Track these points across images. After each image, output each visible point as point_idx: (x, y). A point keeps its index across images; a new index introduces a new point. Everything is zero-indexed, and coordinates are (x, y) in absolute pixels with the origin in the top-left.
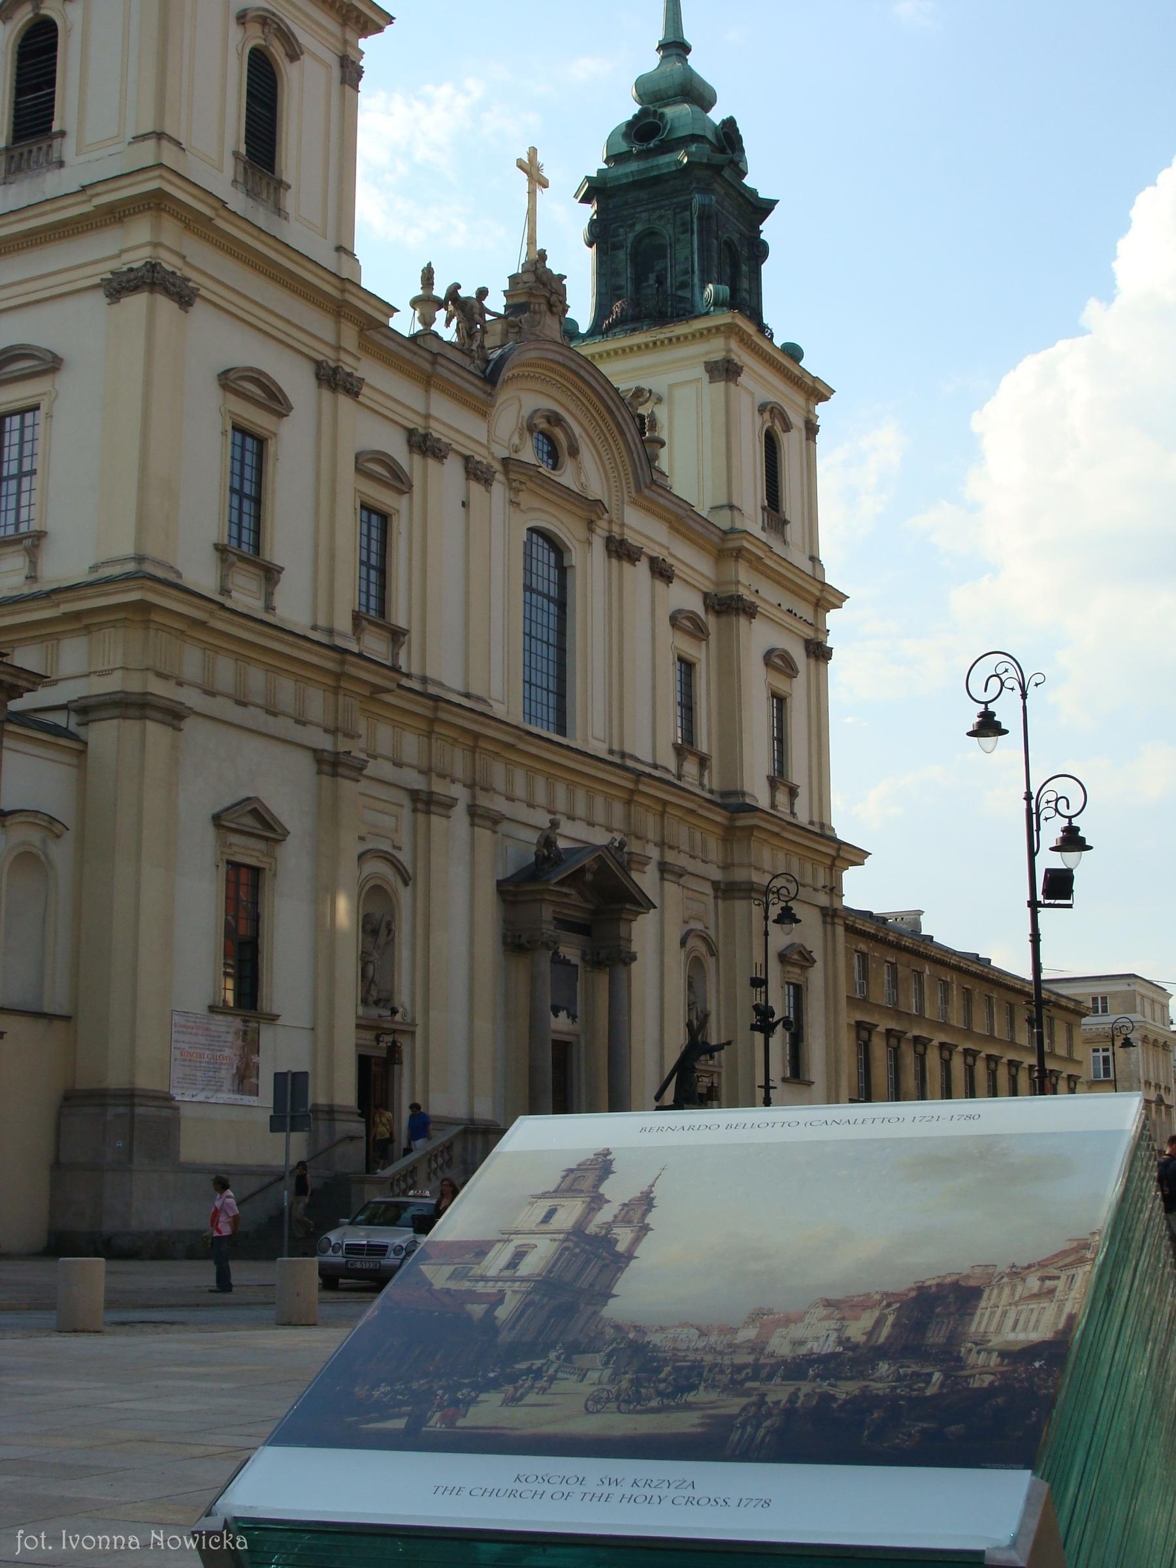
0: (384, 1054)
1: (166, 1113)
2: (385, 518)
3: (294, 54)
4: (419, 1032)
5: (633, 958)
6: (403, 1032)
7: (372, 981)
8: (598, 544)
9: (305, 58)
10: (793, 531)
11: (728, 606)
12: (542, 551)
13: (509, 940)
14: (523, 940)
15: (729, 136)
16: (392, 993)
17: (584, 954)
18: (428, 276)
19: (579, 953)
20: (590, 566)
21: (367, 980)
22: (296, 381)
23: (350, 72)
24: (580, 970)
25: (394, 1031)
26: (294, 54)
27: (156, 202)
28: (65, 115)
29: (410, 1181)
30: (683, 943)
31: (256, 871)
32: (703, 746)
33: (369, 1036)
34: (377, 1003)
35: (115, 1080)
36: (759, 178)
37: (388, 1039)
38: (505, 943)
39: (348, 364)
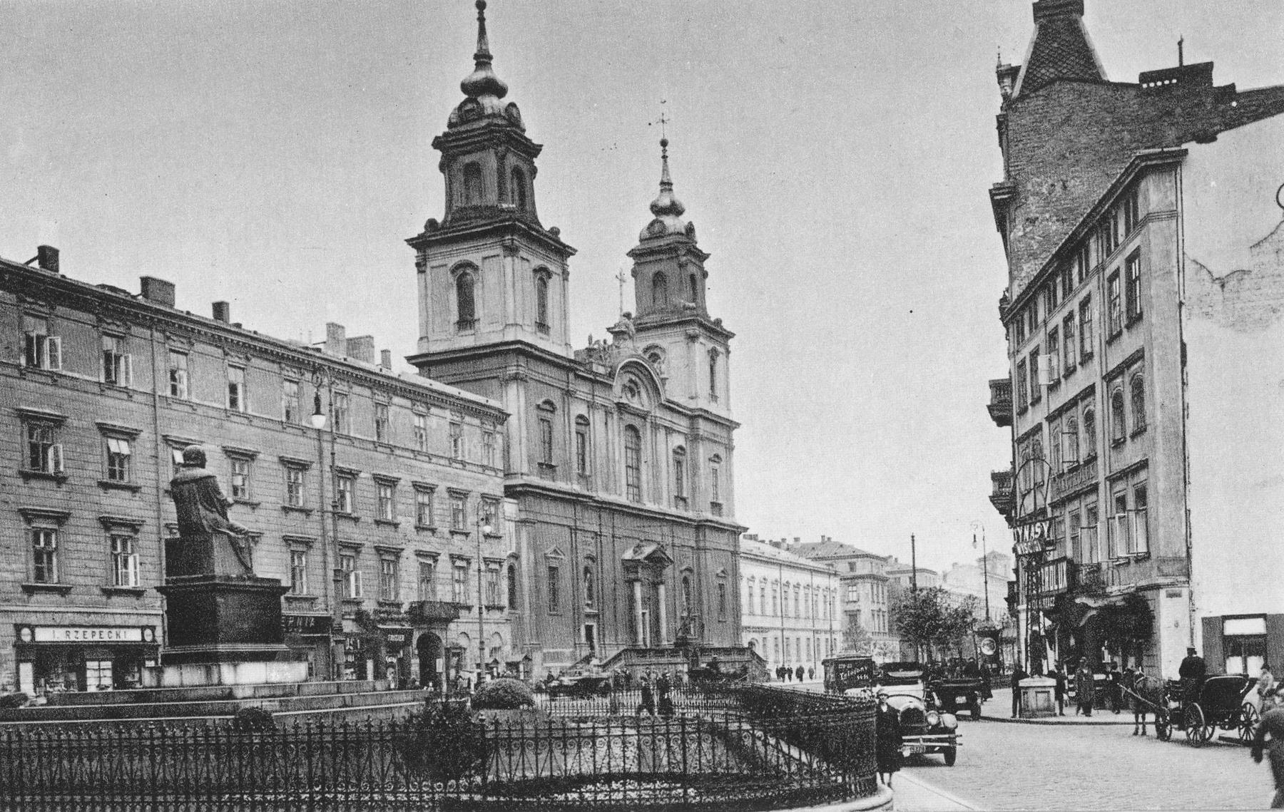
2: (583, 435)
3: (549, 275)
8: (648, 425)
9: (554, 277)
10: (721, 400)
11: (695, 438)
12: (630, 433)
15: (690, 230)
18: (590, 338)
20: (647, 435)
22: (556, 397)
23: (565, 274)
26: (549, 275)
27: (519, 352)
28: (479, 312)
31: (555, 569)
32: (685, 495)
36: (702, 244)
39: (571, 387)
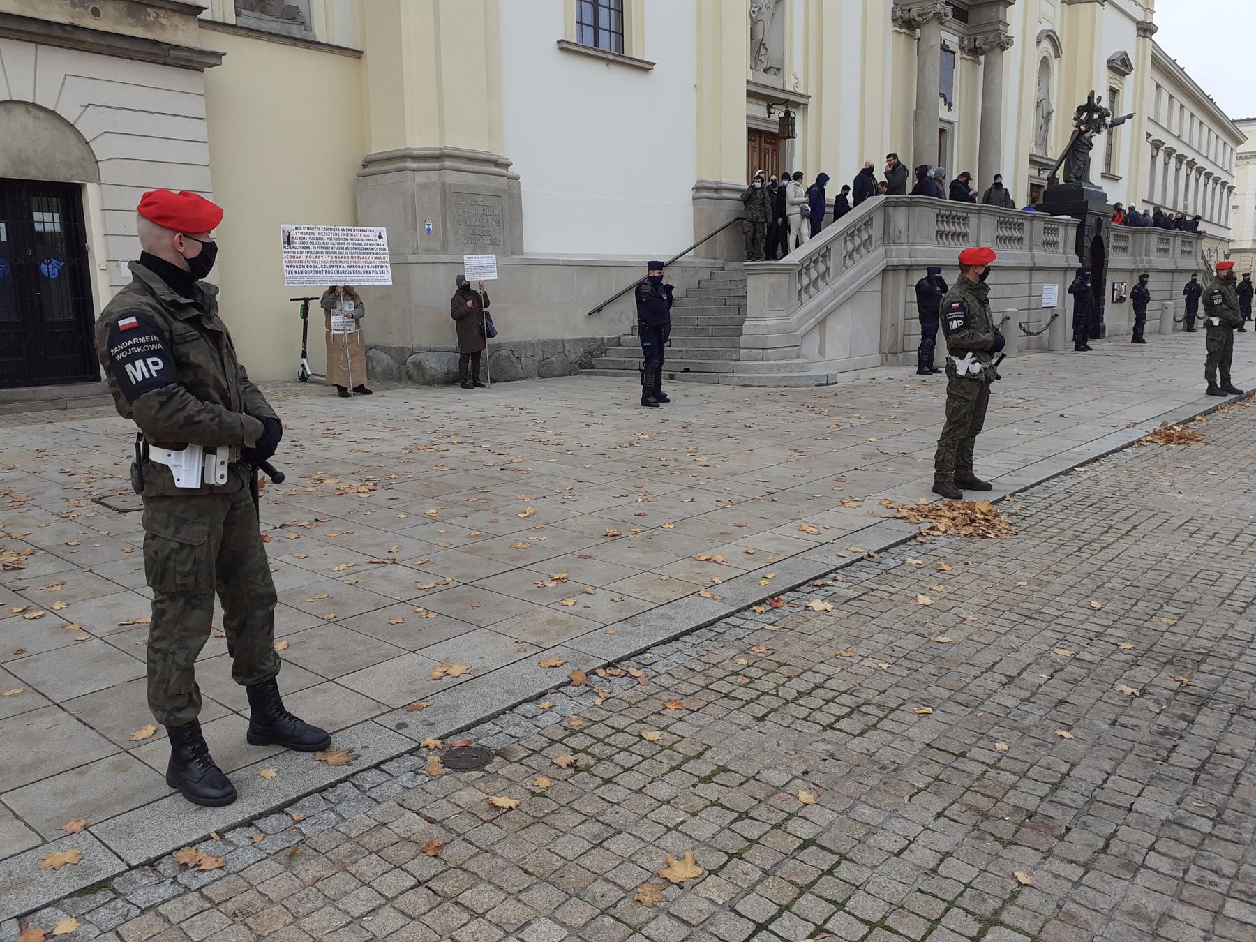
0: (775, 129)
1: (495, 183)
4: (812, 104)
5: (1003, 45)
6: (797, 105)
7: (762, 44)
13: (899, 13)
14: (913, 14)
16: (782, 61)
17: (961, 40)
19: (956, 39)
21: (758, 46)
24: (958, 55)
25: (786, 102)
29: (822, 268)
30: (1039, 42)
33: (760, 110)
34: (765, 71)
35: (421, 140)
37: (778, 113)
38: (894, 20)
